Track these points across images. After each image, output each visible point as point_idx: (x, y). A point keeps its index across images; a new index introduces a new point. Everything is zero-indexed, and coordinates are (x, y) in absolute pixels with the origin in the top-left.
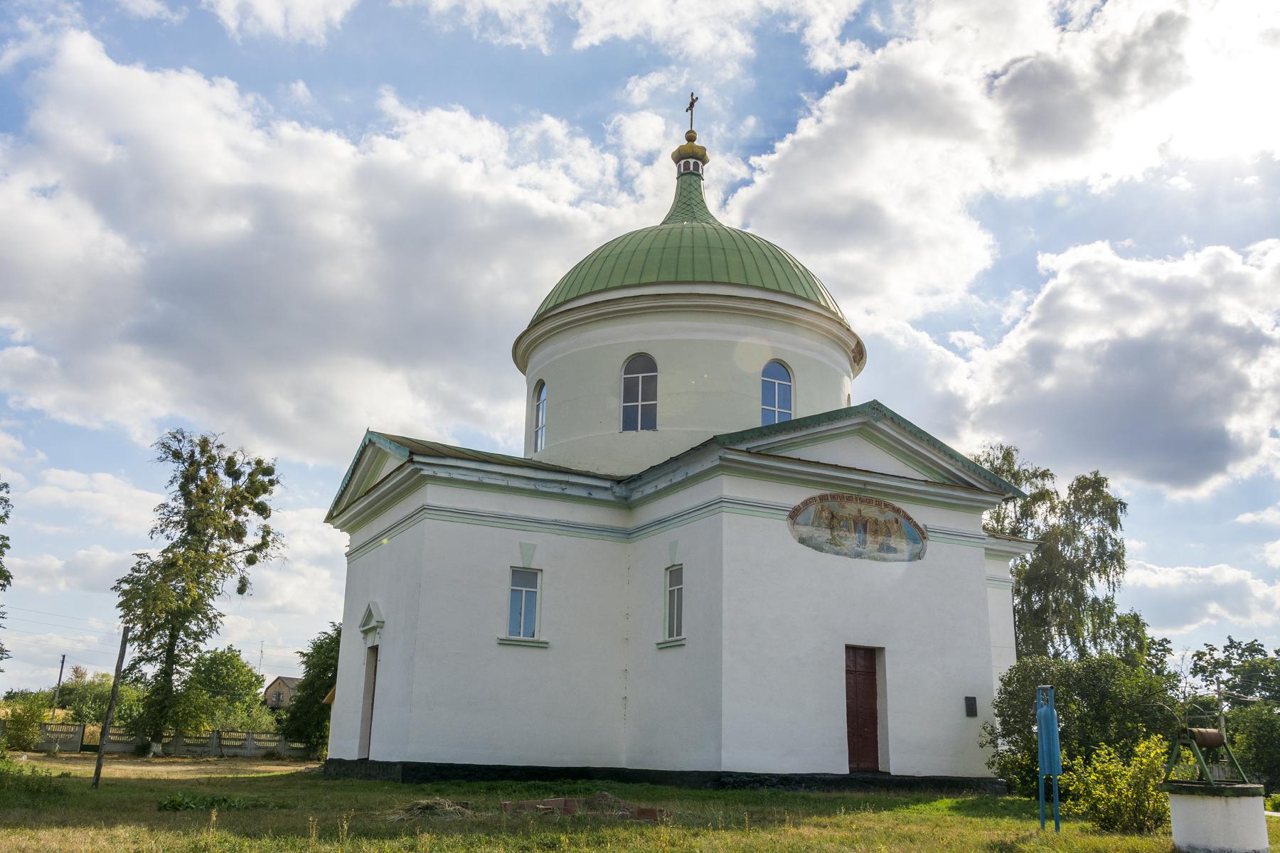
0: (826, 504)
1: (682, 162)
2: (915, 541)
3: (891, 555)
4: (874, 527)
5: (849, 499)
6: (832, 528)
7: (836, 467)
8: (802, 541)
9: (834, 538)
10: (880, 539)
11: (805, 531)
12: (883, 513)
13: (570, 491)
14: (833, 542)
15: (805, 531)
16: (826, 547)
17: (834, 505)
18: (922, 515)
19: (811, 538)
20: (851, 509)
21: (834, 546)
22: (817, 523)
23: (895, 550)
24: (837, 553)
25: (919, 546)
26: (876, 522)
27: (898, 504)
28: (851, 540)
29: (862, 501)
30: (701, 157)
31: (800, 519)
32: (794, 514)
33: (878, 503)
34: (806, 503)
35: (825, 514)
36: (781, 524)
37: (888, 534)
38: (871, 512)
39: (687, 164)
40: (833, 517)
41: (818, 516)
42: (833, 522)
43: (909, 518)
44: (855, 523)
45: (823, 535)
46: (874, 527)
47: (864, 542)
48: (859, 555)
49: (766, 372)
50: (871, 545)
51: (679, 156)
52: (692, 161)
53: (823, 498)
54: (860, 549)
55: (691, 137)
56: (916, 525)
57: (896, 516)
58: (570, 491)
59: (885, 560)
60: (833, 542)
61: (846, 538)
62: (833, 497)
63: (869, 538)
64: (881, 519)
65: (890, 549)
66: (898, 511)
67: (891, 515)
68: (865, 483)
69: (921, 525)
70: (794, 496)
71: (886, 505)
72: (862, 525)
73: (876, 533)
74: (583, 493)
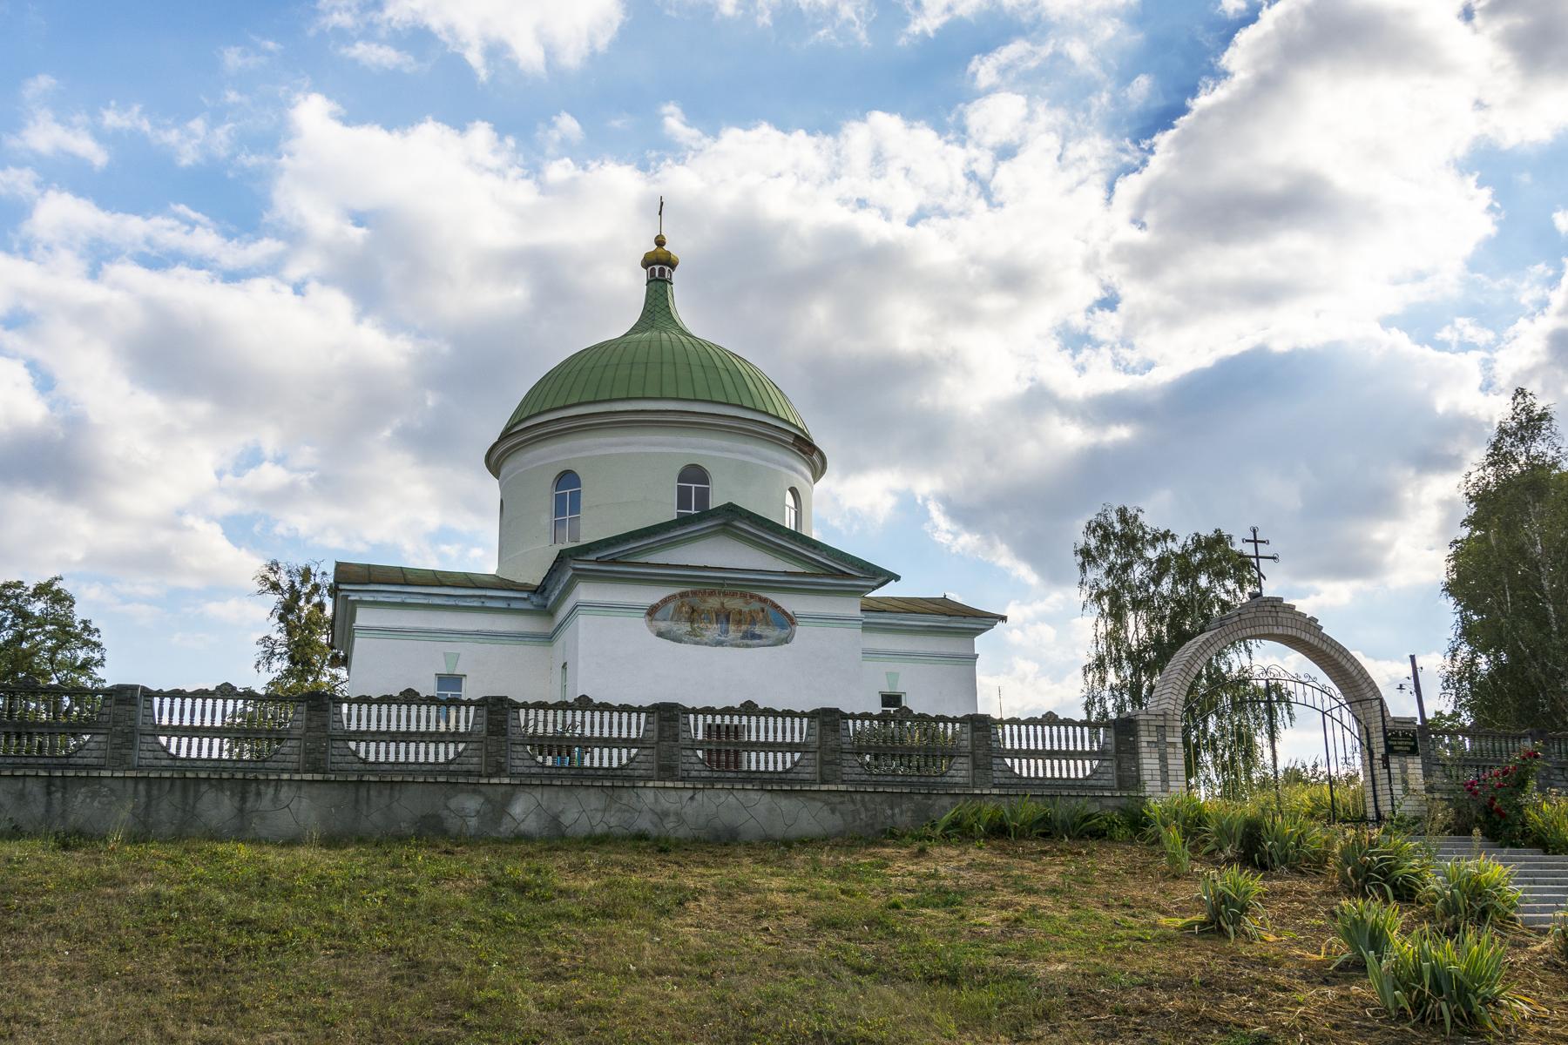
2: (783, 627)
5: (712, 593)
6: (692, 621)
8: (660, 634)
10: (744, 627)
11: (663, 625)
13: (488, 604)
14: (693, 633)
15: (663, 625)
17: (696, 601)
18: (791, 603)
20: (713, 603)
21: (695, 638)
22: (677, 616)
23: (760, 637)
24: (697, 643)
26: (740, 612)
27: (764, 595)
28: (713, 631)
29: (725, 594)
31: (657, 615)
32: (652, 612)
33: (743, 595)
34: (665, 601)
36: (639, 623)
37: (753, 622)
38: (734, 604)
41: (678, 611)
42: (693, 615)
43: (777, 607)
45: (685, 627)
47: (727, 632)
48: (720, 644)
49: (682, 477)
50: (734, 632)
51: (648, 262)
53: (682, 595)
55: (660, 242)
56: (785, 613)
58: (488, 604)
59: (748, 646)
60: (693, 633)
61: (707, 629)
62: (694, 593)
63: (732, 627)
64: (746, 609)
65: (754, 636)
66: (765, 601)
67: (756, 605)
70: (652, 595)
71: (752, 596)
72: (724, 616)
73: (739, 622)
74: (503, 605)
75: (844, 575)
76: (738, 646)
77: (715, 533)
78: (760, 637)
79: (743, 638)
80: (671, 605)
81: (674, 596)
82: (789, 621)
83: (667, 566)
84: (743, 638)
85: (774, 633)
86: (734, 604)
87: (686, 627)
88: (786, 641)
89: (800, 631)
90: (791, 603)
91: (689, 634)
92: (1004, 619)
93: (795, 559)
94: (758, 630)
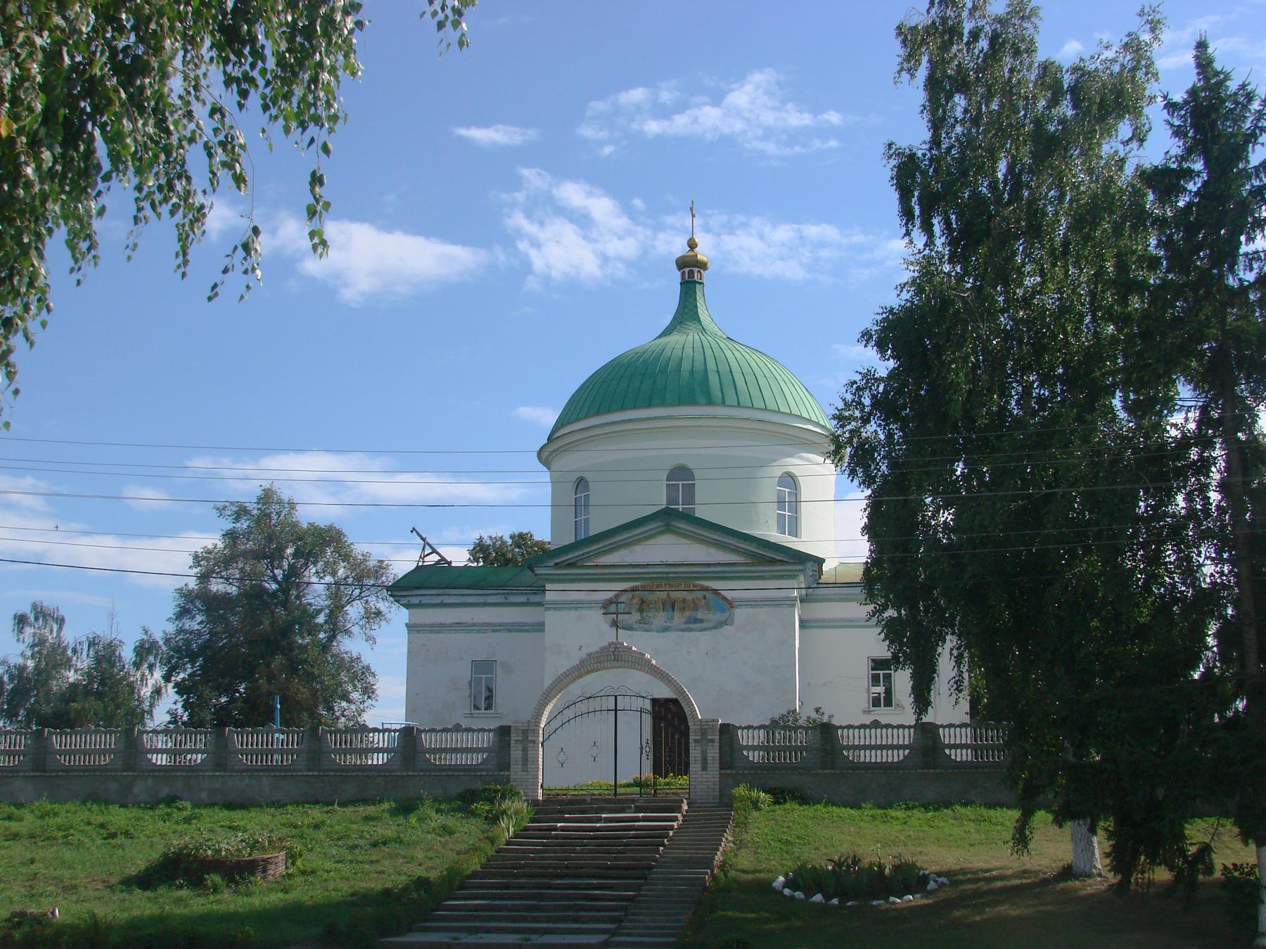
1: (687, 270)
2: (723, 611)
3: (698, 625)
6: (641, 610)
7: (631, 566)
10: (687, 614)
23: (702, 621)
24: (646, 630)
25: (727, 615)
26: (684, 601)
28: (660, 618)
32: (606, 605)
37: (696, 608)
39: (691, 273)
40: (643, 602)
42: (643, 606)
48: (666, 629)
52: (696, 270)
53: (633, 590)
59: (691, 630)
65: (696, 621)
67: (700, 594)
70: (606, 591)
72: (670, 605)
73: (683, 609)
76: (683, 630)
77: (661, 533)
78: (702, 621)
79: (686, 623)
82: (730, 604)
84: (686, 623)
85: (719, 617)
87: (636, 616)
88: (725, 623)
89: (740, 614)
93: (733, 550)
94: (700, 615)
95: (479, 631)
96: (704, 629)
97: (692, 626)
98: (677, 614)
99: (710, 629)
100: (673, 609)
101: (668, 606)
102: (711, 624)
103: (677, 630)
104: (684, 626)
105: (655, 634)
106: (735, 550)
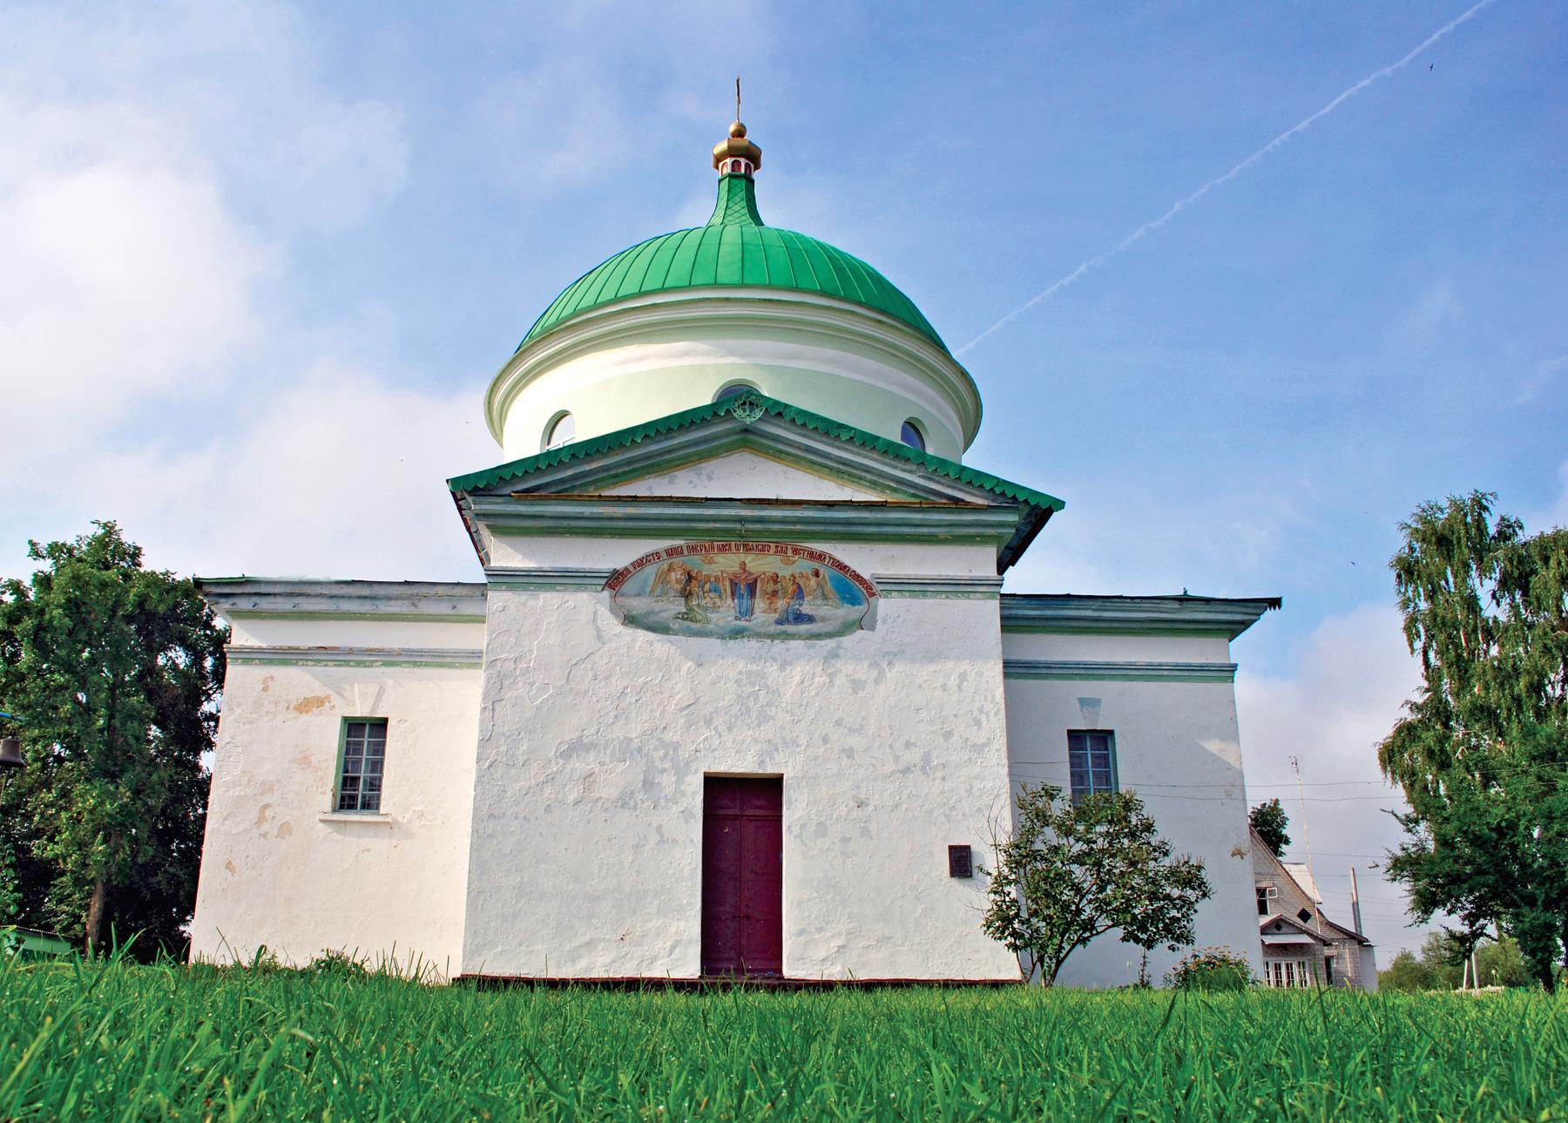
0: (678, 560)
2: (854, 601)
3: (803, 628)
4: (770, 587)
6: (686, 595)
8: (631, 620)
9: (691, 609)
10: (781, 604)
12: (788, 562)
14: (685, 617)
15: (638, 605)
16: (676, 625)
17: (695, 562)
19: (648, 614)
20: (727, 563)
21: (689, 624)
22: (660, 588)
23: (810, 619)
24: (698, 634)
25: (862, 608)
26: (775, 579)
28: (725, 613)
30: (753, 157)
31: (629, 586)
32: (615, 580)
33: (781, 551)
34: (640, 563)
35: (676, 576)
40: (690, 578)
41: (662, 578)
43: (843, 567)
44: (734, 584)
46: (770, 587)
48: (737, 634)
50: (762, 614)
53: (671, 552)
54: (742, 623)
56: (857, 577)
57: (816, 565)
61: (715, 608)
64: (785, 572)
65: (800, 618)
66: (820, 557)
67: (804, 566)
68: (741, 520)
69: (866, 576)
72: (745, 587)
73: (775, 593)
75: (957, 505)
76: (772, 637)
77: (730, 449)
78: (810, 619)
80: (651, 571)
81: (657, 555)
83: (619, 499)
86: (763, 564)
88: (859, 624)
89: (886, 606)
90: (865, 560)
91: (685, 617)
92: (1275, 603)
94: (806, 609)
95: (359, 664)
96: (818, 636)
97: (790, 628)
98: (760, 604)
99: (829, 635)
100: (752, 593)
101: (743, 588)
102: (829, 627)
103: (760, 636)
104: (774, 628)
105: (713, 643)
106: (876, 480)
